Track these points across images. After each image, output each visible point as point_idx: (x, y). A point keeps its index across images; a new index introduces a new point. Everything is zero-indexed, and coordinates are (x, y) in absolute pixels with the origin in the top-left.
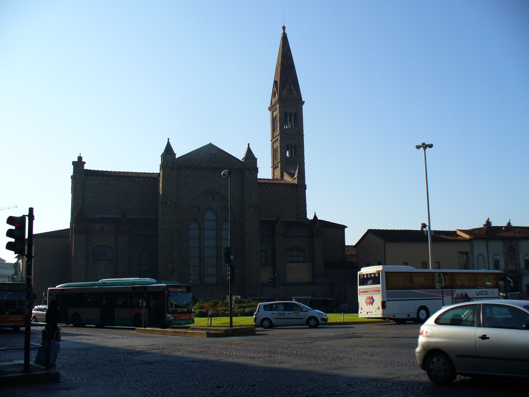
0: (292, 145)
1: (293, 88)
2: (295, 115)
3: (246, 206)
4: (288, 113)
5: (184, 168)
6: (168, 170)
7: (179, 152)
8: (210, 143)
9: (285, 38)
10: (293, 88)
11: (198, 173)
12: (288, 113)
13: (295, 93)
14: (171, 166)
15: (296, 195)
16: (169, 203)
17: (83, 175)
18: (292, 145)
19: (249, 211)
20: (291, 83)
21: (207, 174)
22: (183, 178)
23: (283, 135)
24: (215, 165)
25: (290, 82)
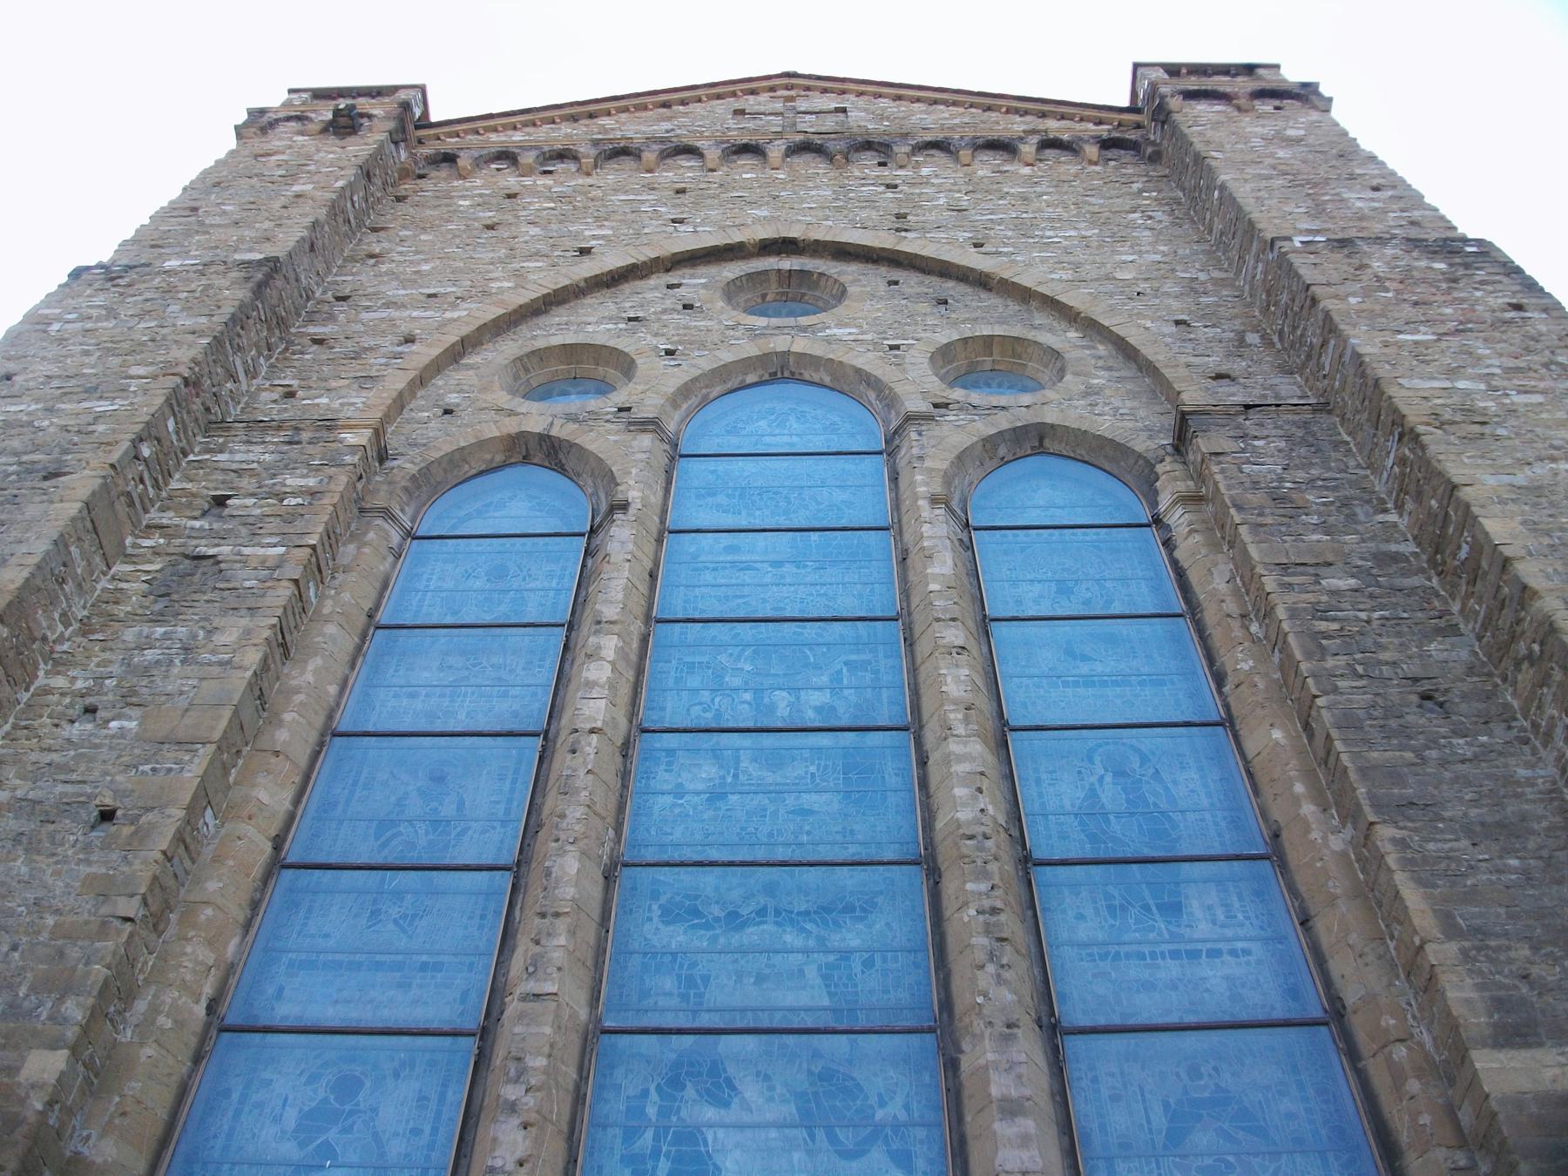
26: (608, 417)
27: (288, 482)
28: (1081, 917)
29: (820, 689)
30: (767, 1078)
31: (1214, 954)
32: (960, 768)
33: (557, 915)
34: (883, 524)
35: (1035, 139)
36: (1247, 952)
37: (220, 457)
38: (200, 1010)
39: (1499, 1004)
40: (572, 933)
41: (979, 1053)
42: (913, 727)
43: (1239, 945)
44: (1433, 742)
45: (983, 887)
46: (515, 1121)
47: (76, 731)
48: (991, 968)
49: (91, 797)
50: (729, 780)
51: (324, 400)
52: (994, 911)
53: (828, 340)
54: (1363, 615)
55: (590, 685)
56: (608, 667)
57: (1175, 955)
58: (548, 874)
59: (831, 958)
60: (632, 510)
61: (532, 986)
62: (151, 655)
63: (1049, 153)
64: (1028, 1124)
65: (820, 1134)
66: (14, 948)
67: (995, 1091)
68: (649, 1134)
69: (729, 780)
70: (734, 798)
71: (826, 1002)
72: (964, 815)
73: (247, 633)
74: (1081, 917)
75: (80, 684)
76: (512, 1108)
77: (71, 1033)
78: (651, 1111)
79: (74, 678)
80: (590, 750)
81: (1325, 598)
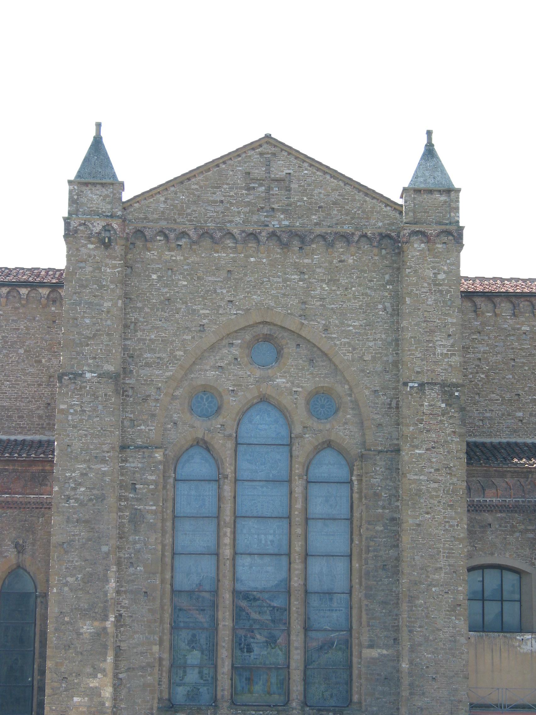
5: (158, 238)
6: (91, 246)
8: (268, 136)
11: (216, 255)
14: (99, 233)
16: (88, 375)
19: (422, 405)
21: (252, 259)
22: (154, 277)
24: (287, 223)
26: (219, 430)
27: (148, 477)
28: (314, 601)
29: (271, 534)
30: (261, 634)
31: (336, 610)
32: (297, 572)
33: (226, 608)
34: (287, 480)
35: (358, 233)
36: (342, 610)
37: (128, 465)
38: (169, 625)
39: (371, 640)
40: (229, 611)
41: (293, 638)
42: (289, 555)
43: (341, 609)
44: (381, 580)
45: (297, 603)
46: (225, 649)
47: (131, 570)
48: (297, 621)
49: (142, 589)
50: (253, 562)
51: (143, 427)
52: (298, 608)
53: (278, 386)
54: (380, 540)
55: (226, 545)
56: (229, 539)
57: (329, 610)
58: (224, 598)
59: (271, 609)
60: (229, 478)
61: (224, 623)
62: (138, 546)
63: (363, 239)
64: (299, 651)
65: (269, 645)
66: (142, 626)
67: (295, 645)
68: (243, 644)
69: (253, 562)
70: (254, 568)
71: (270, 618)
72: (296, 585)
73: (156, 539)
74: (314, 601)
75: (126, 556)
76: (224, 647)
77: (158, 643)
78: (243, 640)
79: (124, 554)
80: (227, 565)
81: (374, 534)
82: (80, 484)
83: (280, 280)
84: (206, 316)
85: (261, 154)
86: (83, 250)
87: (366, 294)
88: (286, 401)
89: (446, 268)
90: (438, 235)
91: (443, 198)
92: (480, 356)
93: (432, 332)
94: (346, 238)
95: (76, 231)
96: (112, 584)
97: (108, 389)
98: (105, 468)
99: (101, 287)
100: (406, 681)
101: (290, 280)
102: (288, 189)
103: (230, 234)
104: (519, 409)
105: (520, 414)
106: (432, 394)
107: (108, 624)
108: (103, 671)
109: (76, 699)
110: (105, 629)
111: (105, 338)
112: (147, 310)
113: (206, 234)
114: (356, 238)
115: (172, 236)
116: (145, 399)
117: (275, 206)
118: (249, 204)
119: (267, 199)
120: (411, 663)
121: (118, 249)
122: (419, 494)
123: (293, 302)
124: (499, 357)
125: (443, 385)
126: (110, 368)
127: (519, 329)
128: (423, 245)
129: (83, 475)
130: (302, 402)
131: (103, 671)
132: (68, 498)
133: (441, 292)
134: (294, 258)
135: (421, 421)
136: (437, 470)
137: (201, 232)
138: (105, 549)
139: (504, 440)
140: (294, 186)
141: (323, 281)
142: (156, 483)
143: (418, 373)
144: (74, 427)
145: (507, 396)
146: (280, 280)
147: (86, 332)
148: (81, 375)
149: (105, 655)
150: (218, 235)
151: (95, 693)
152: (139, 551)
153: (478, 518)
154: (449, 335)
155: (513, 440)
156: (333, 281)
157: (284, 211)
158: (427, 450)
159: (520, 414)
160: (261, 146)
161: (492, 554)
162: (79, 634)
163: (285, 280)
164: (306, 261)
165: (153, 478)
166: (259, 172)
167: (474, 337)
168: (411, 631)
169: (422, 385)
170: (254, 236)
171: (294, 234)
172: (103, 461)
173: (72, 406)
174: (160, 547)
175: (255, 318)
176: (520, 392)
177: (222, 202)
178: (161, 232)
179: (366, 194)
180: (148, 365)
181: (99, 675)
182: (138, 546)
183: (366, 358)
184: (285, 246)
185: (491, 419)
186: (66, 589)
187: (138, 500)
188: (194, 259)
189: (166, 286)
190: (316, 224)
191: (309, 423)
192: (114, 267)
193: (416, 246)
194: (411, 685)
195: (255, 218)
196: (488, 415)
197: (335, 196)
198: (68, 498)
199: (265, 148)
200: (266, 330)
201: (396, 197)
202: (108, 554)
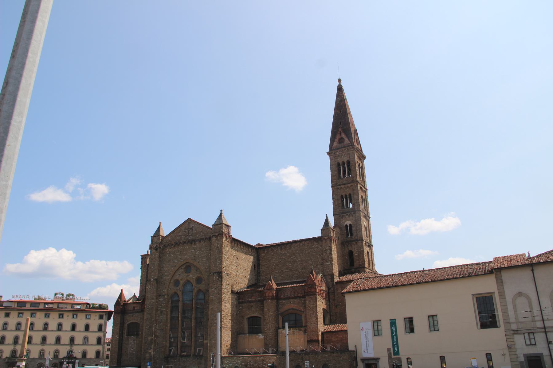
0: (346, 195)
1: (343, 136)
2: (348, 162)
3: (210, 273)
4: (341, 162)
7: (165, 232)
9: (340, 89)
10: (344, 136)
12: (341, 162)
13: (347, 140)
15: (322, 249)
16: (152, 280)
17: (146, 265)
18: (346, 195)
20: (341, 132)
21: (185, 248)
23: (336, 187)
24: (192, 238)
25: (340, 131)
35: (205, 238)
47: (160, 324)
62: (162, 319)
82: (149, 305)
83: (190, 252)
84: (176, 263)
85: (188, 223)
86: (153, 252)
87: (207, 252)
88: (191, 281)
89: (220, 243)
90: (218, 235)
91: (220, 226)
92: (273, 262)
93: (216, 259)
94: (203, 239)
95: (152, 247)
96: (154, 328)
97: (155, 283)
98: (154, 301)
99: (155, 259)
100: (209, 348)
101: (192, 251)
102: (193, 230)
103: (181, 243)
104: (282, 274)
105: (283, 275)
106: (216, 275)
107: (153, 337)
108: (152, 348)
109: (147, 355)
110: (152, 338)
111: (155, 271)
112: (166, 263)
113: (176, 244)
114: (204, 239)
115: (170, 245)
116: (165, 284)
117: (190, 234)
118: (185, 235)
119: (188, 233)
120: (210, 344)
121: (159, 250)
122: (212, 300)
123: (193, 257)
124: (278, 261)
125: (218, 272)
126: (156, 278)
127: (282, 253)
128: (215, 238)
129: (150, 303)
130: (194, 280)
131: (152, 348)
132: (147, 308)
133: (218, 249)
134: (193, 246)
135: (213, 282)
136: (216, 294)
137: (175, 243)
138: (153, 320)
139: (279, 282)
140: (194, 229)
141: (198, 250)
142: (165, 303)
143: (213, 270)
144: (149, 292)
145: (280, 271)
146: (190, 252)
147: (152, 270)
148: (151, 280)
149: (152, 344)
150: (179, 243)
151: (150, 353)
152: (161, 320)
153: (250, 304)
154: (220, 260)
155: (281, 282)
156: (200, 250)
157: (191, 235)
158: (214, 289)
159: (283, 275)
160: (188, 221)
161: (253, 313)
162: (148, 340)
163: (191, 252)
164: (195, 246)
165: (165, 302)
166: (187, 227)
167: (272, 257)
168: (210, 336)
169: (214, 273)
170: (185, 242)
171: (192, 240)
172: (153, 299)
173: (149, 287)
174: (165, 319)
175: (185, 262)
176: (282, 269)
177: (180, 235)
178: (168, 245)
179: (208, 228)
180: (165, 276)
181: (151, 349)
182: (162, 319)
183: (206, 268)
184: (191, 243)
185: (276, 277)
186: (146, 330)
187: (162, 308)
188: (174, 250)
189: (169, 257)
190: (198, 237)
191: (196, 286)
192: (158, 254)
193: (214, 238)
194: (210, 349)
195: (186, 238)
196: (275, 276)
197: (202, 230)
198: (147, 308)
199: (189, 221)
200: (188, 264)
201: (211, 227)
202: (153, 321)
